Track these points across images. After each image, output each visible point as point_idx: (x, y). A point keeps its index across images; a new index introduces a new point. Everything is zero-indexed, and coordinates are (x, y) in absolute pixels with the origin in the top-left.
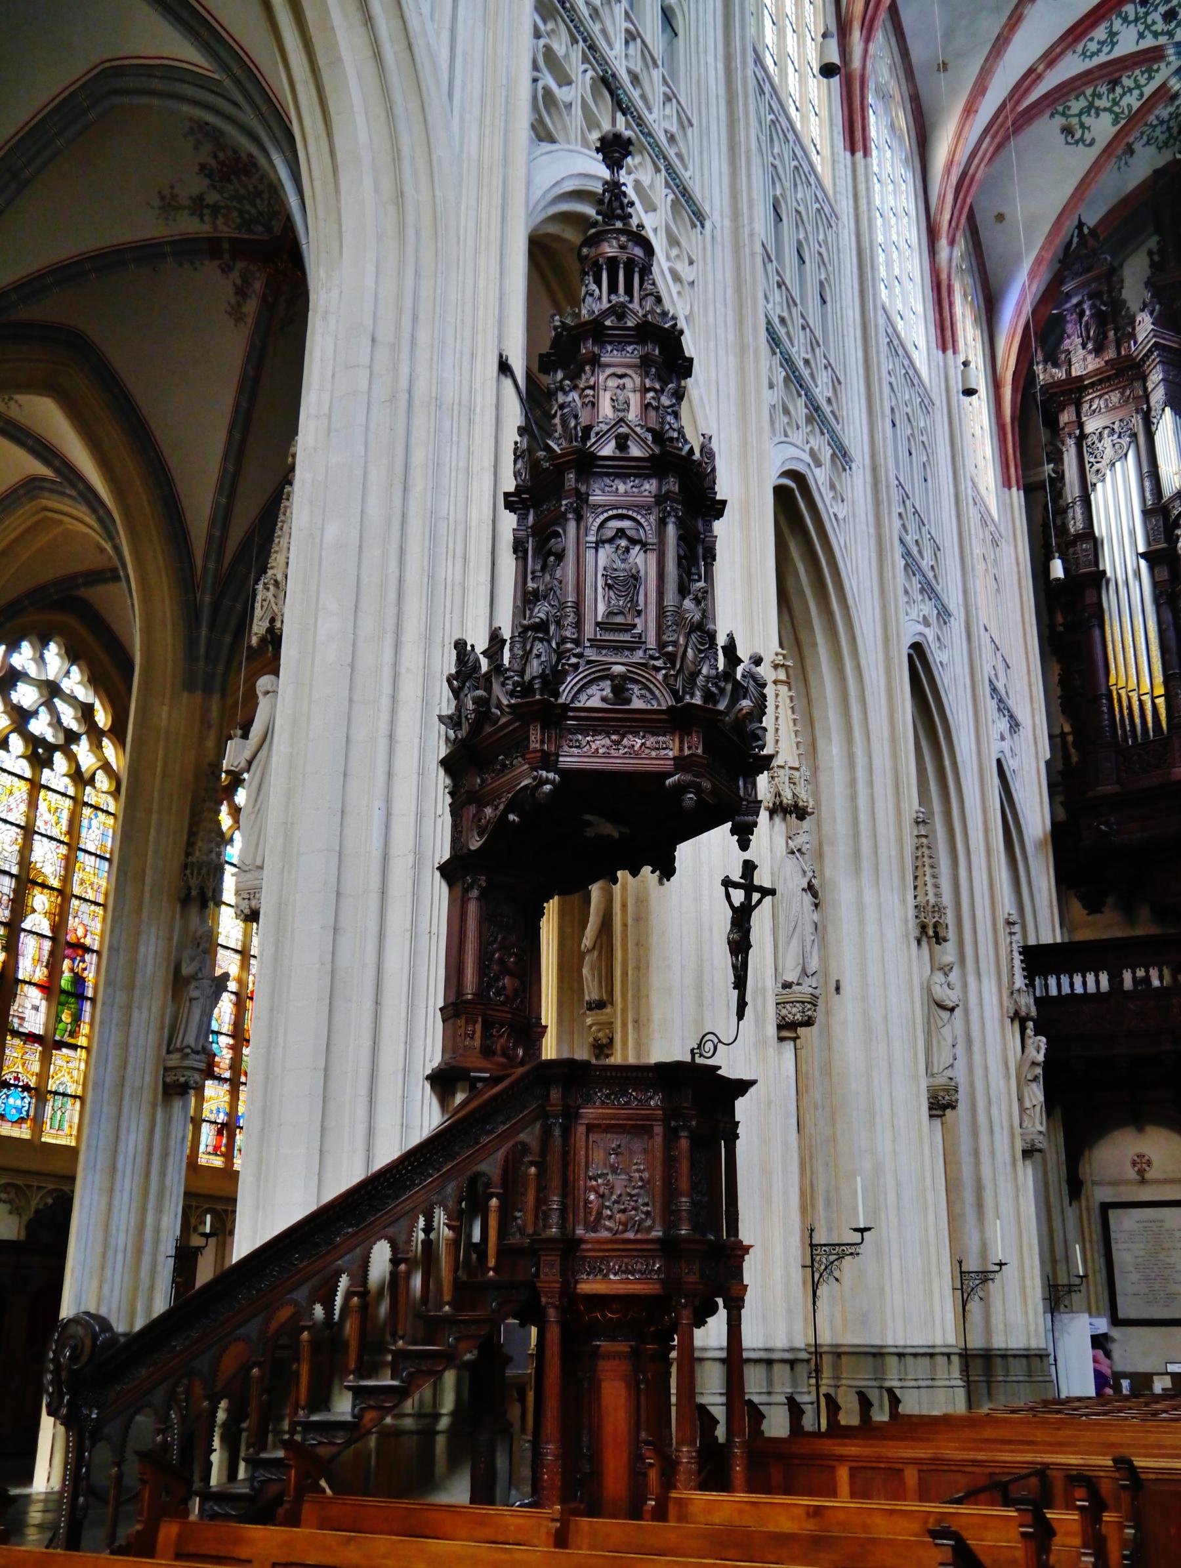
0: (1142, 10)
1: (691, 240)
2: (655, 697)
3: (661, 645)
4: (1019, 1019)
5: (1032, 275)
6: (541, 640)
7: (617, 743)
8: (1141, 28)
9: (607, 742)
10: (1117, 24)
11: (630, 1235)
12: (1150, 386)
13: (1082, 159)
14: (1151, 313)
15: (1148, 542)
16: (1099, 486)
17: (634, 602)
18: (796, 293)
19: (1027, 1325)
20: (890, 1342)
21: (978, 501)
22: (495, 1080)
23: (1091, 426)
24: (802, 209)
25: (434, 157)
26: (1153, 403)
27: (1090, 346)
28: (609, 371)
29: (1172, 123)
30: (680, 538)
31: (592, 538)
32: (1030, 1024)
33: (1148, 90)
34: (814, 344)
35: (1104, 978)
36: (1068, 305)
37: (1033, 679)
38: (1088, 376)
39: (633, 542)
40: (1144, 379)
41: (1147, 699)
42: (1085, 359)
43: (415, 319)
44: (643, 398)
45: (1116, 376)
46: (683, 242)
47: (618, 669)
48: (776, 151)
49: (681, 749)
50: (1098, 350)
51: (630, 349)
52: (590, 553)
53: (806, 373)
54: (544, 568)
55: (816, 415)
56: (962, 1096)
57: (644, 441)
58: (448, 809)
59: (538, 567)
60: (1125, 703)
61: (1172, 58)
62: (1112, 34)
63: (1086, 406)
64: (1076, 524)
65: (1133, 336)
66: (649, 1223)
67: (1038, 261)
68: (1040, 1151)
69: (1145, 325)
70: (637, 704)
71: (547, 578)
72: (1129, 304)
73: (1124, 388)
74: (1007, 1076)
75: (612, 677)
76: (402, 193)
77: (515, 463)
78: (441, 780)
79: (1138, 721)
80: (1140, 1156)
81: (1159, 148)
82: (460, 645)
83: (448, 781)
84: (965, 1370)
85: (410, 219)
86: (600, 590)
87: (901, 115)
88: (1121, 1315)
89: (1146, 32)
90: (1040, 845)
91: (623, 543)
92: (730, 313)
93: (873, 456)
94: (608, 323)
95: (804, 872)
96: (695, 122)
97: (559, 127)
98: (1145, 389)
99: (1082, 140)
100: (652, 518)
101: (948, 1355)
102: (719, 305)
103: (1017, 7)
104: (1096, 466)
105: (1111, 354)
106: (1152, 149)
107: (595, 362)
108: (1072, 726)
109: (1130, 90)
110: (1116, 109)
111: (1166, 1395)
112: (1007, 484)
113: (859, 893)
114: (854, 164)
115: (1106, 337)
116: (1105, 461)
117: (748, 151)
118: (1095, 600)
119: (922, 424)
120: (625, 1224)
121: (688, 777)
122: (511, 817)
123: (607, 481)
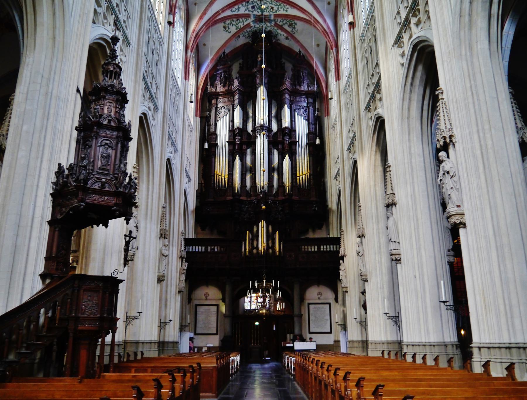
0: (247, 4)
1: (126, 50)
2: (111, 188)
3: (114, 174)
4: (182, 258)
5: (211, 62)
6: (84, 170)
7: (101, 198)
8: (246, 8)
9: (98, 197)
10: (240, 6)
11: (92, 316)
12: (235, 99)
13: (226, 36)
15: (229, 139)
16: (219, 121)
17: (108, 162)
18: (150, 64)
19: (174, 335)
20: (141, 340)
21: (189, 120)
22: (60, 278)
23: (220, 105)
24: (155, 40)
25: (65, 30)
26: (235, 103)
27: (222, 85)
28: (108, 101)
30: (121, 147)
31: (99, 144)
32: (184, 259)
33: (246, 23)
34: (153, 78)
35: (204, 248)
36: (218, 72)
37: (196, 168)
38: (221, 92)
39: (109, 147)
40: (234, 96)
41: (223, 178)
42: (220, 88)
43: (55, 73)
44: (116, 109)
45: (227, 94)
46: (124, 51)
47: (104, 180)
48: (150, 24)
49: (116, 201)
50: (224, 86)
51: (114, 96)
52: (98, 148)
53: (150, 85)
54: (85, 148)
55: (151, 98)
56: (166, 278)
57: (115, 121)
58: (51, 206)
59: (83, 148)
60: (218, 178)
61: (252, 18)
62: (239, 8)
64: (212, 130)
65: (233, 85)
66: (96, 313)
67: (212, 59)
68: (183, 291)
69: (236, 83)
70: (107, 189)
71: (85, 151)
73: (229, 98)
74: (177, 272)
75: (102, 182)
76: (55, 38)
77: (79, 119)
78: (50, 198)
79: (220, 183)
80: (207, 293)
82: (60, 165)
83: (52, 199)
84: (159, 346)
85: (56, 46)
86: (100, 157)
87: (183, 14)
88: (197, 332)
90: (192, 212)
91: (107, 147)
92: (134, 71)
93: (164, 109)
94: (109, 89)
95: (135, 222)
96: (131, 17)
97: (97, 19)
98: (234, 99)
99: (228, 31)
100: (115, 141)
101: (155, 343)
102: (131, 69)
104: (219, 116)
105: (227, 88)
106: (244, 38)
107: (104, 98)
108: (204, 182)
109: (241, 22)
111: (206, 352)
112: (196, 115)
113: (146, 224)
114: (170, 29)
115: (226, 83)
116: (222, 115)
117: (144, 28)
118: (214, 151)
119: (177, 99)
120: (91, 313)
121: (118, 208)
122: (71, 212)
123: (105, 130)
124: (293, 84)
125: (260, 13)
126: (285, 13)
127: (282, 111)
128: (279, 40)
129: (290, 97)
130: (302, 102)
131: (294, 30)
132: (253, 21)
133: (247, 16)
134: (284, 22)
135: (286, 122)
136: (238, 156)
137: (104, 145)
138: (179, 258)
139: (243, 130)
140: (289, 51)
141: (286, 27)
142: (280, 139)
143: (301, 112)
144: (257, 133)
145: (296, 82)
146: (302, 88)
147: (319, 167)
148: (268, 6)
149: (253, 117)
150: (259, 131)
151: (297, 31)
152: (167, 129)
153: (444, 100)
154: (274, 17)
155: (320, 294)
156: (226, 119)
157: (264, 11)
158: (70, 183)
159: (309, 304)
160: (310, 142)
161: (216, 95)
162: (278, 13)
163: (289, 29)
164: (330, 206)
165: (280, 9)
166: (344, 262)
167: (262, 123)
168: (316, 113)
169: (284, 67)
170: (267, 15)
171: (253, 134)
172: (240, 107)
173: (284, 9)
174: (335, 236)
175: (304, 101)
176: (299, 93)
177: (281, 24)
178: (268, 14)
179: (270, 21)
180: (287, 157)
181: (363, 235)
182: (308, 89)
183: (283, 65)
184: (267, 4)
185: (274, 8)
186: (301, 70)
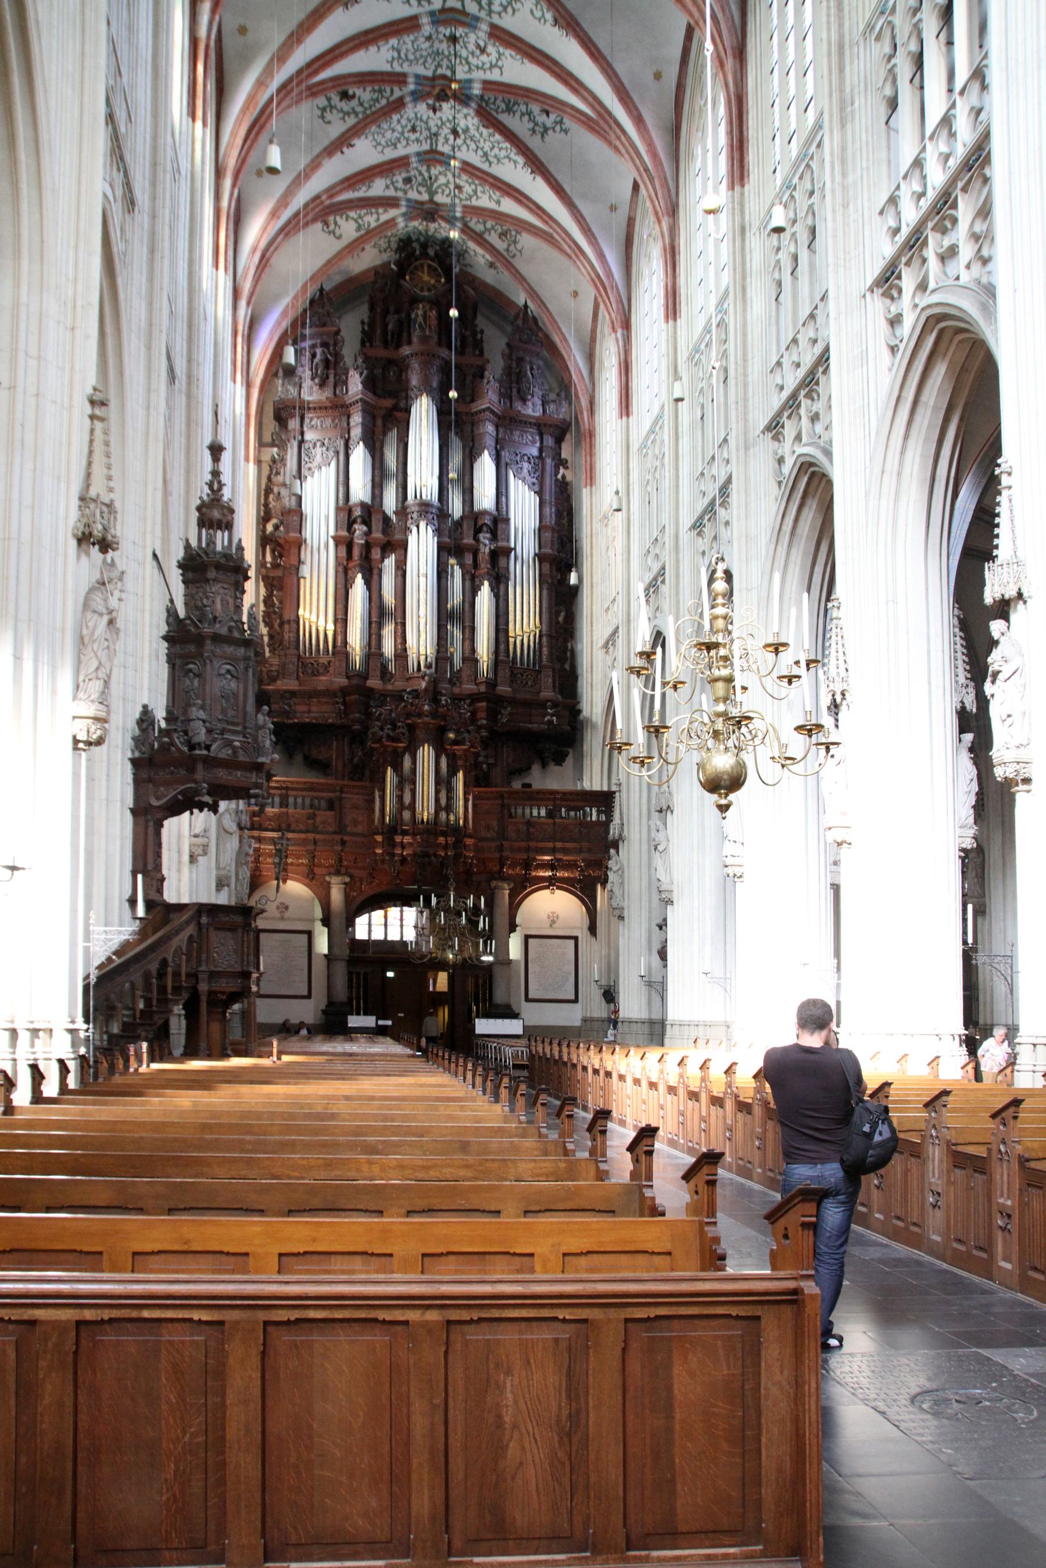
8: (389, 182)
12: (352, 424)
13: (335, 246)
29: (392, 239)
33: (384, 217)
45: (331, 408)
65: (345, 383)
69: (355, 385)
72: (346, 359)
75: (234, 748)
81: (380, 252)
89: (391, 186)
91: (229, 676)
98: (348, 424)
106: (375, 251)
110: (360, 221)
124: (506, 395)
125: (425, 197)
126: (492, 206)
127: (476, 466)
128: (471, 266)
129: (497, 431)
130: (527, 444)
132: (404, 215)
133: (390, 202)
134: (489, 225)
135: (485, 497)
137: (223, 675)
139: (370, 511)
141: (493, 238)
142: (468, 540)
143: (525, 471)
144: (410, 521)
145: (515, 391)
146: (529, 411)
147: (563, 614)
148: (448, 182)
149: (400, 476)
153: (841, 622)
154: (464, 212)
157: (437, 193)
160: (543, 550)
161: (302, 409)
162: (474, 202)
163: (500, 245)
164: (586, 712)
165: (479, 194)
167: (424, 497)
169: (482, 341)
171: (399, 520)
173: (490, 197)
174: (596, 787)
176: (520, 422)
177: (479, 228)
178: (448, 200)
179: (451, 221)
180: (486, 588)
181: (669, 807)
183: (479, 336)
184: (446, 175)
185: (465, 190)
186: (528, 359)
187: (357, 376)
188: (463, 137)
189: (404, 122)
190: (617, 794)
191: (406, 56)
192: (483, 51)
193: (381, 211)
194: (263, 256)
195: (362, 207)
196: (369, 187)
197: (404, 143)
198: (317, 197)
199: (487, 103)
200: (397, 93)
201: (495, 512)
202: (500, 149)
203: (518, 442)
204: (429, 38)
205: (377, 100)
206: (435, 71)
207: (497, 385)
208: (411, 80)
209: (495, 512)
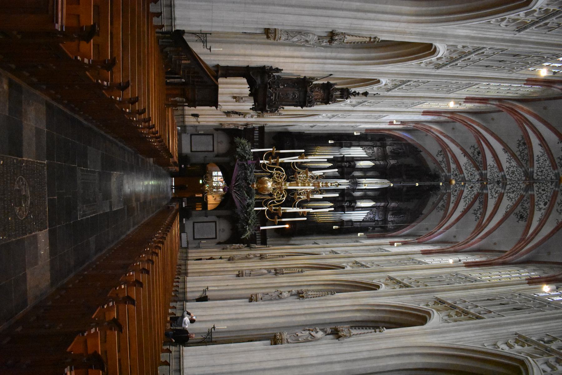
4: (247, 125)
8: (455, 169)
12: (380, 161)
14: (396, 164)
16: (362, 149)
23: (375, 149)
27: (392, 150)
28: (323, 94)
33: (444, 169)
35: (257, 139)
36: (403, 146)
38: (386, 150)
47: (272, 98)
50: (391, 152)
63: (380, 148)
64: (354, 143)
65: (393, 159)
69: (392, 162)
70: (267, 99)
71: (291, 84)
82: (282, 70)
90: (286, 129)
98: (380, 160)
99: (438, 154)
103: (460, 145)
104: (366, 149)
105: (389, 154)
107: (324, 92)
114: (421, 112)
116: (367, 150)
126: (451, 201)
127: (370, 200)
131: (439, 209)
132: (446, 175)
133: (449, 170)
134: (445, 201)
136: (332, 165)
138: (246, 123)
140: (423, 205)
145: (395, 211)
146: (389, 217)
148: (457, 187)
150: (353, 181)
151: (439, 211)
152: (340, 114)
154: (449, 192)
155: (224, 230)
156: (363, 154)
158: (270, 79)
159: (215, 222)
162: (452, 196)
164: (293, 238)
165: (454, 197)
166: (246, 247)
168: (371, 228)
170: (450, 187)
172: (373, 166)
173: (454, 200)
175: (380, 218)
176: (386, 214)
177: (444, 198)
182: (390, 221)
187: (395, 162)
188: (471, 190)
189: (473, 172)
190: (266, 246)
191: (492, 170)
192: (496, 193)
193: (446, 168)
194: (428, 130)
195: (447, 162)
196: (453, 163)
197: (467, 172)
198: (448, 147)
199: (482, 195)
200: (481, 168)
201: (356, 206)
202: (468, 201)
203: (379, 213)
204: (498, 176)
205: (478, 162)
206: (489, 179)
207: (397, 206)
208: (485, 172)
209: (356, 206)
